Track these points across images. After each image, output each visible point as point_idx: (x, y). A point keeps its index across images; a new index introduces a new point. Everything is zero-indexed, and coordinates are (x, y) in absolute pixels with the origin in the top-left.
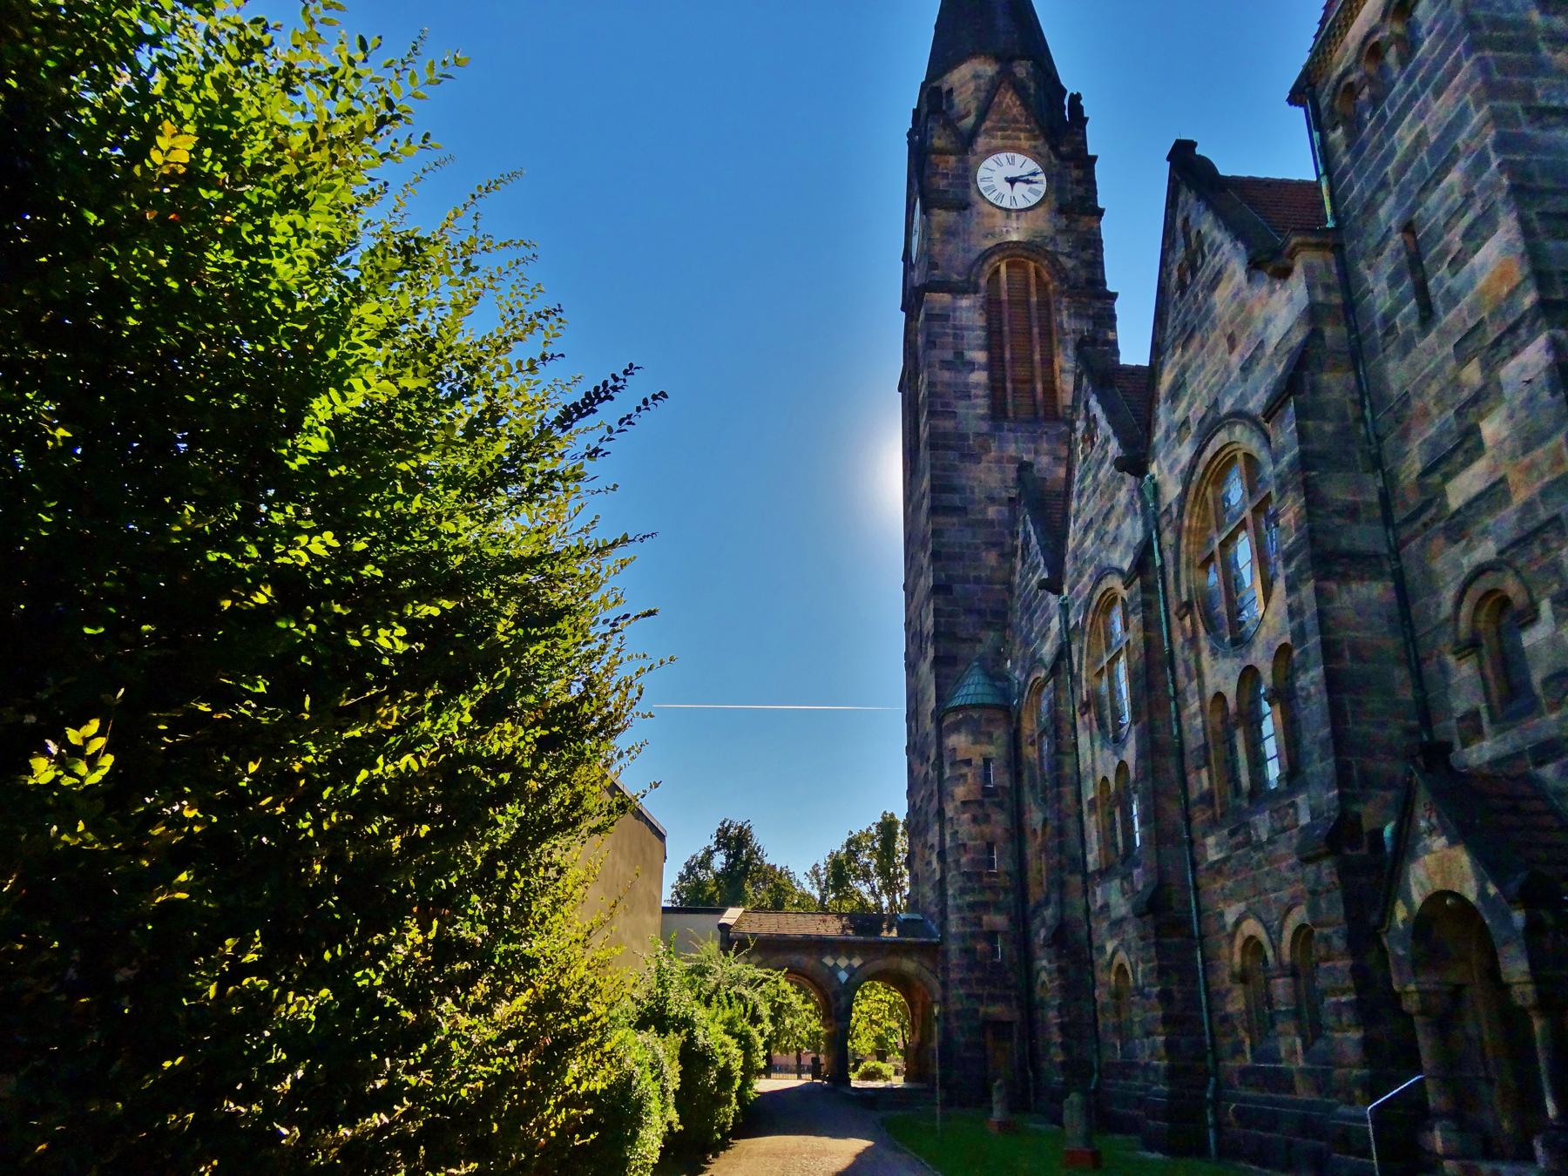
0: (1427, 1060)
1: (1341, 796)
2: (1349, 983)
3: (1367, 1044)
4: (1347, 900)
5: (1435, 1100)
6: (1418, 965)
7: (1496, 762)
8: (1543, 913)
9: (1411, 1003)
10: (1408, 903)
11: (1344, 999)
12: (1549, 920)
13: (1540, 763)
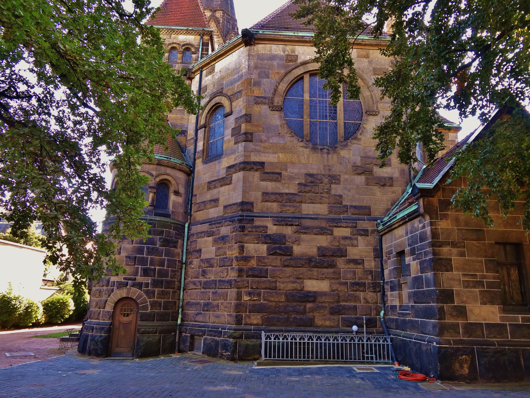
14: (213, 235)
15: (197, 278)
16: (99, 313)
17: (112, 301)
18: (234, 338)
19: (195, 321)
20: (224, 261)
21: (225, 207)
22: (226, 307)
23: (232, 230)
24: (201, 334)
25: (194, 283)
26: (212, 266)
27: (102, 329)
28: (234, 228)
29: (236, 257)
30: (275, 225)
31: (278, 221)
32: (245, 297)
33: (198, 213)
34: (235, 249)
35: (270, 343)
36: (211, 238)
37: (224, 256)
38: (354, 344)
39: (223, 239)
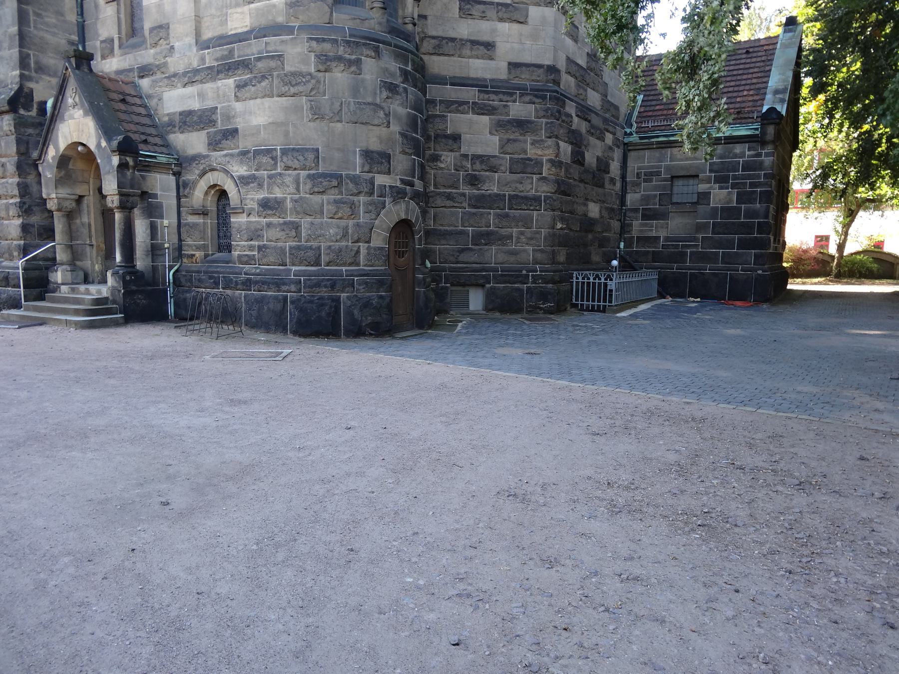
0: (58, 236)
1: (22, 76)
2: (16, 192)
3: (25, 228)
4: (19, 142)
5: (61, 256)
6: (59, 182)
7: (119, 72)
8: (128, 159)
9: (51, 205)
10: (57, 148)
11: (11, 201)
12: (131, 163)
13: (142, 77)
14: (493, 114)
15: (456, 188)
16: (358, 252)
17: (384, 226)
18: (554, 283)
19: (457, 263)
20: (524, 163)
21: (514, 66)
22: (531, 239)
23: (542, 113)
24: (481, 281)
25: (449, 197)
26: (493, 169)
27: (381, 283)
28: (546, 110)
29: (551, 161)
30: (577, 116)
31: (581, 111)
32: (558, 224)
33: (435, 58)
34: (548, 147)
35: (600, 284)
36: (485, 119)
37: (521, 156)
38: (589, 283)
39: (521, 125)
